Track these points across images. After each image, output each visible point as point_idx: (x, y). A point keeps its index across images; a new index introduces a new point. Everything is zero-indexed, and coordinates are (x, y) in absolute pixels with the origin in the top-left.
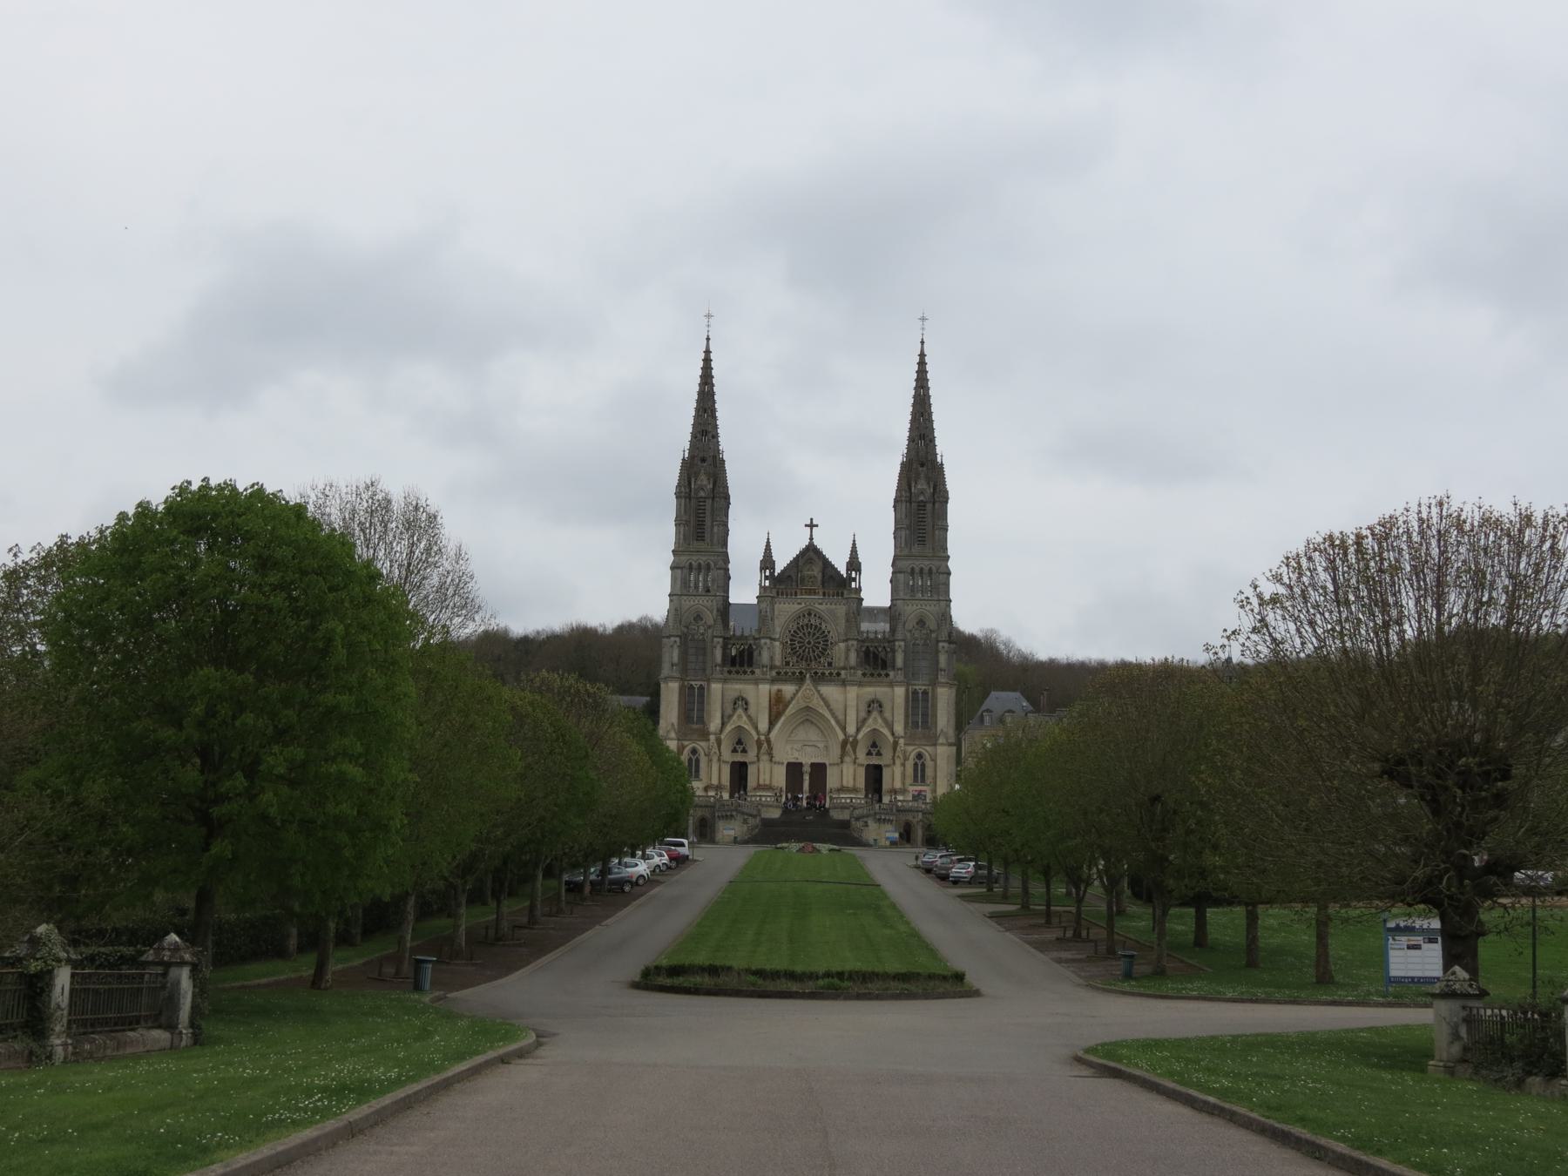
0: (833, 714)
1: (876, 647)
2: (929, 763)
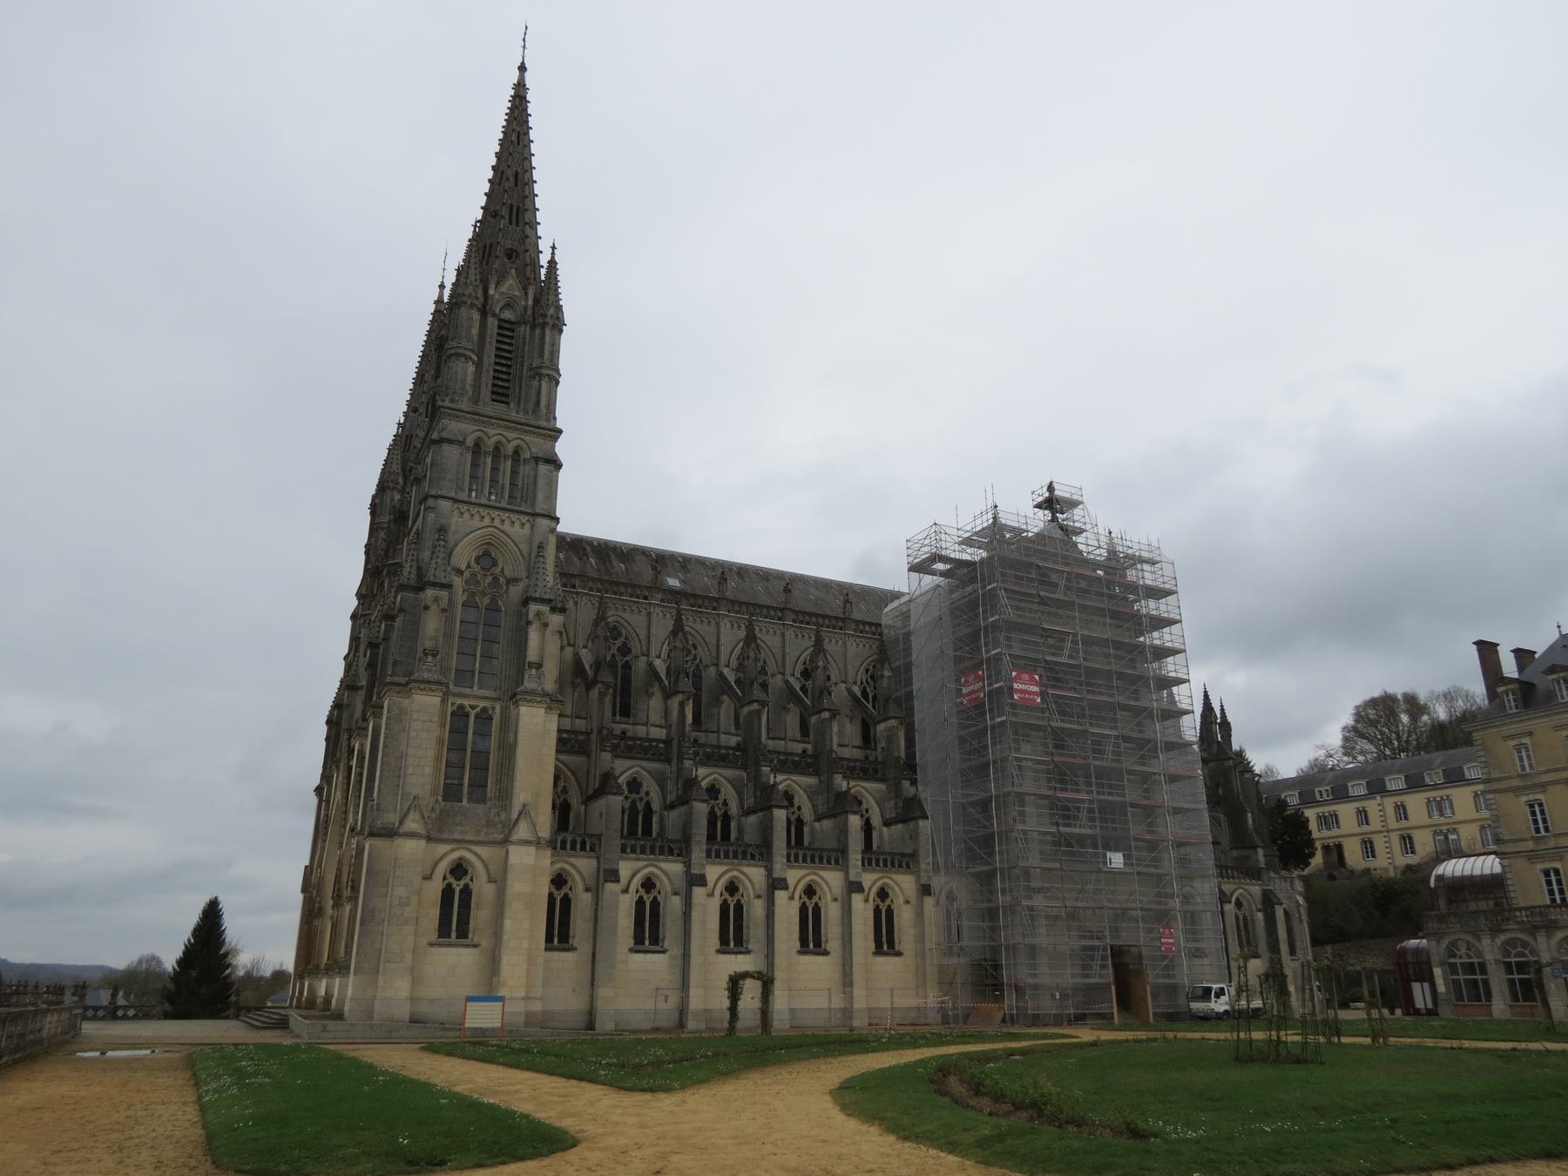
2: (483, 890)
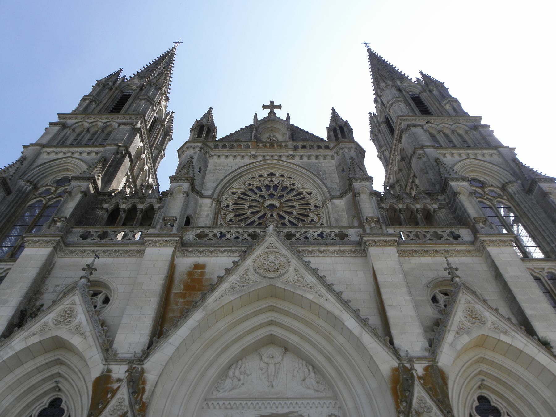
0: (346, 304)
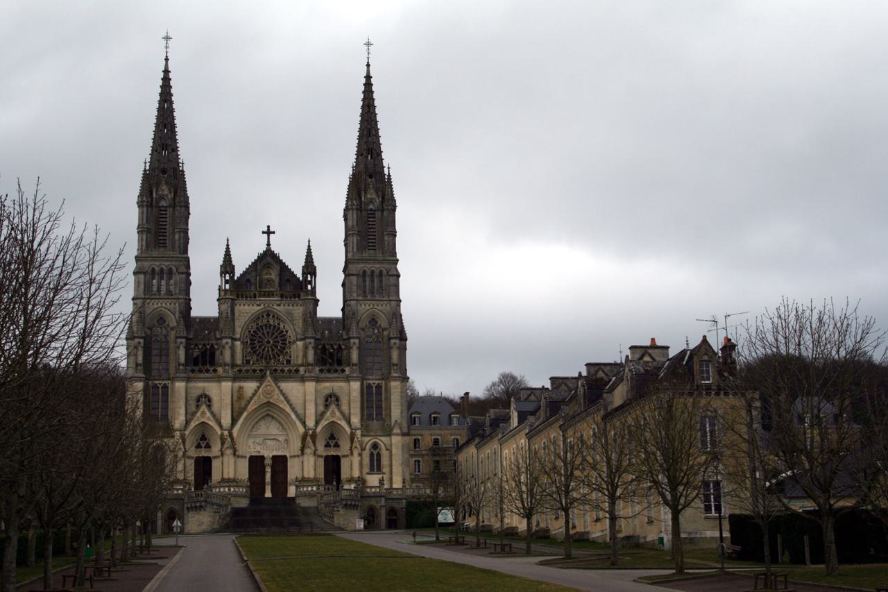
0: (293, 409)
1: (332, 345)
2: (384, 453)
